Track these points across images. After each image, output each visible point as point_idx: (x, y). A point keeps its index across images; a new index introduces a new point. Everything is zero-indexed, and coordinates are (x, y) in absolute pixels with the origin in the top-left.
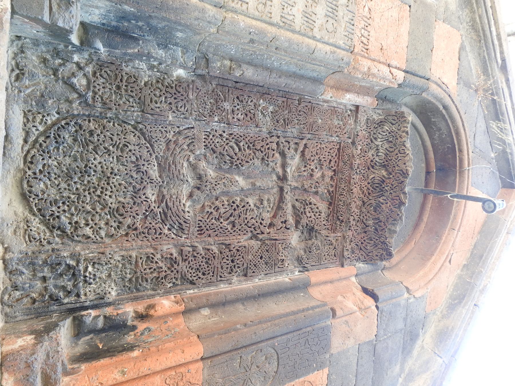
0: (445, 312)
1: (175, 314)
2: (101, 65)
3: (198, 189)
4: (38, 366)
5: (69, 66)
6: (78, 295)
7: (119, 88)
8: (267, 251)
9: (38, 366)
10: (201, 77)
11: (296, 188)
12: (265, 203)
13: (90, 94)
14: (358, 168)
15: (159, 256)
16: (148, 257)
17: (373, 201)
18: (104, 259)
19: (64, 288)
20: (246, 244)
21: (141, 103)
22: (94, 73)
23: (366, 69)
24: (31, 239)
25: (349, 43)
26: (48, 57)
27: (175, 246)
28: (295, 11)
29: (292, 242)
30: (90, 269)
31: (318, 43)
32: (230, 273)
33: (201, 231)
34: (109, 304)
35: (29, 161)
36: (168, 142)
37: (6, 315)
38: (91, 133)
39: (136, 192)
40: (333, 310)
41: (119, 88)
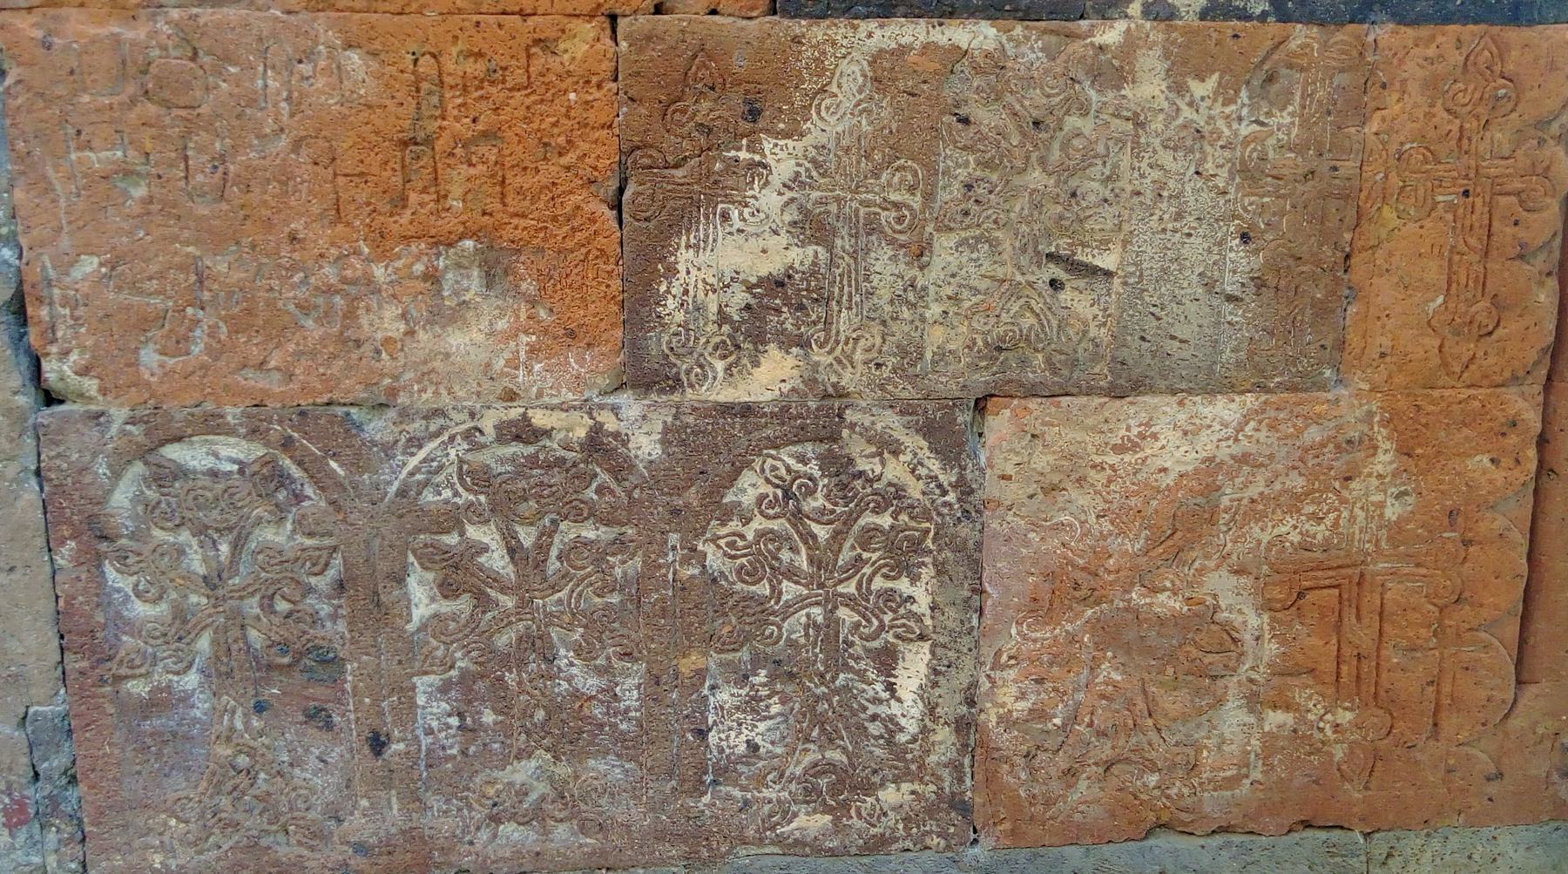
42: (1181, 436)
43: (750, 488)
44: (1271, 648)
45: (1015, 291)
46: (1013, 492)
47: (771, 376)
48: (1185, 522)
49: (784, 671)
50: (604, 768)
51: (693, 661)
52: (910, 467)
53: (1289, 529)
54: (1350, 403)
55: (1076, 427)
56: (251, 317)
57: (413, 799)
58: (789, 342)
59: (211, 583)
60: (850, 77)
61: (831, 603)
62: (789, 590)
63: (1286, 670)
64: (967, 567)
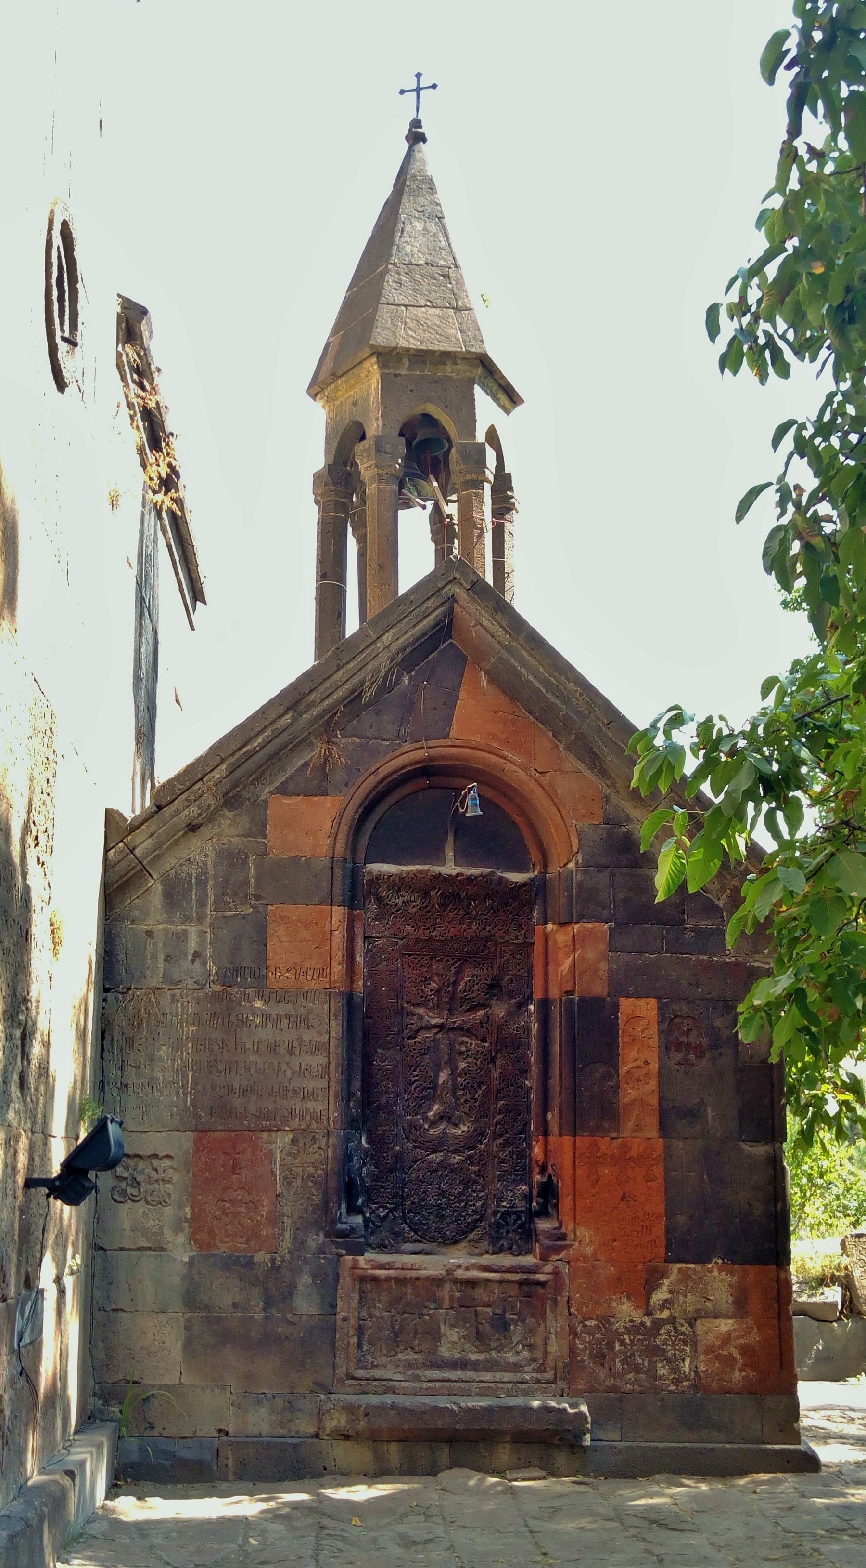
0: (609, 782)
1: (546, 1142)
2: (369, 1200)
3: (450, 1118)
4: (550, 1243)
5: (373, 1219)
6: (521, 1212)
7: (382, 1187)
8: (506, 1047)
9: (550, 1243)
10: (364, 1123)
11: (450, 1010)
12: (463, 1049)
13: (388, 1205)
14: (428, 929)
15: (501, 1154)
16: (502, 1162)
17: (466, 902)
18: (500, 1195)
19: (515, 1221)
20: (499, 1071)
21: (391, 1171)
22: (376, 1203)
23: (340, 967)
24: (481, 1239)
25: (322, 996)
26: (370, 1231)
27: (494, 1140)
28: (314, 1065)
29: (501, 1016)
30: (504, 1204)
31: (332, 1035)
32: (522, 1088)
33: (485, 1116)
34: (531, 1191)
35: (433, 1240)
36: (415, 1147)
37: (526, 1253)
38: (413, 1203)
39: (452, 1171)
40: (567, 993)
41: (382, 1187)
42: (725, 1325)
43: (663, 1331)
44: (741, 1361)
45: (699, 1302)
46: (700, 1333)
47: (665, 1314)
48: (726, 1339)
49: (669, 1361)
50: (643, 1376)
51: (655, 1359)
52: (685, 1329)
53: (742, 1341)
54: (750, 1321)
55: (709, 1323)
56: (597, 1303)
57: (615, 1380)
58: (668, 1309)
59: (589, 1342)
60: (675, 1272)
61: (675, 1350)
62: (669, 1348)
63: (744, 1365)
64: (694, 1345)
